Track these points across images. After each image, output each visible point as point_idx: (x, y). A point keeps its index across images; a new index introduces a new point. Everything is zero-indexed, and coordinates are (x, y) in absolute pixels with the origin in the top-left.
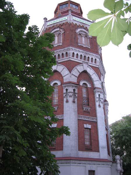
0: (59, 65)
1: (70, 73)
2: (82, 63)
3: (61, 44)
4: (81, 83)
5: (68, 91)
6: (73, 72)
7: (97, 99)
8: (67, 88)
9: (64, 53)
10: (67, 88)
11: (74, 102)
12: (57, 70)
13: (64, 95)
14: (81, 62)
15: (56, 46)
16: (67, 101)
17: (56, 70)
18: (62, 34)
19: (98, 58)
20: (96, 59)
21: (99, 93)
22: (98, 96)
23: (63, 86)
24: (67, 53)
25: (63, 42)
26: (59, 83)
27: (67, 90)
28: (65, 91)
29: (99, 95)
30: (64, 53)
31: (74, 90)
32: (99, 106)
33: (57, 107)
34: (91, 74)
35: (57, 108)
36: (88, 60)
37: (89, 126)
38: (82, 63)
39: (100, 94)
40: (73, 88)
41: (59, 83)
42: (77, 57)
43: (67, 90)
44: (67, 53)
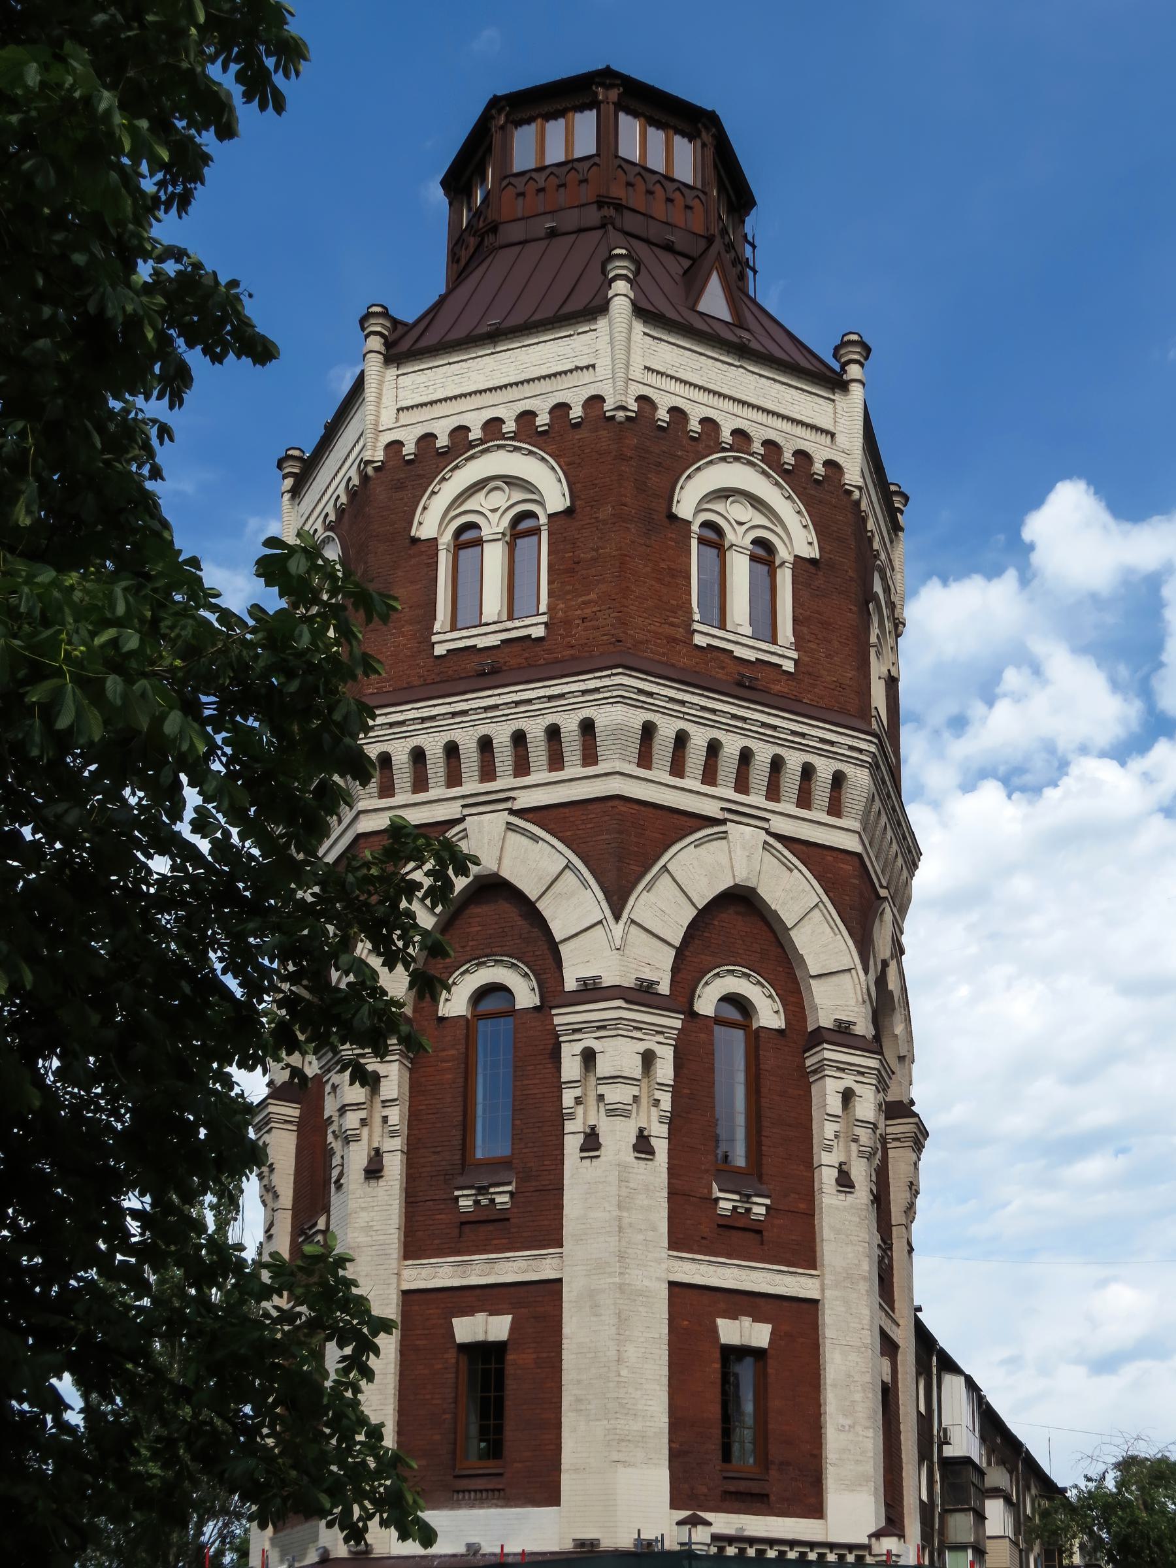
0: (524, 832)
1: (617, 918)
2: (723, 822)
3: (539, 632)
4: (707, 1002)
5: (603, 1067)
7: (830, 1129)
9: (570, 724)
11: (643, 1146)
12: (505, 874)
13: (568, 1098)
14: (710, 808)
15: (493, 640)
16: (591, 1142)
18: (543, 520)
19: (861, 764)
20: (838, 779)
21: (849, 1081)
22: (834, 1104)
23: (557, 1021)
24: (587, 727)
25: (551, 608)
26: (525, 995)
27: (589, 1057)
28: (571, 1067)
29: (848, 1096)
30: (570, 724)
31: (648, 1058)
32: (845, 1181)
34: (789, 920)
36: (773, 793)
37: (758, 1334)
38: (723, 822)
39: (858, 1089)
40: (641, 1047)
41: (525, 995)
42: (678, 768)
43: (589, 1057)
44: (587, 727)
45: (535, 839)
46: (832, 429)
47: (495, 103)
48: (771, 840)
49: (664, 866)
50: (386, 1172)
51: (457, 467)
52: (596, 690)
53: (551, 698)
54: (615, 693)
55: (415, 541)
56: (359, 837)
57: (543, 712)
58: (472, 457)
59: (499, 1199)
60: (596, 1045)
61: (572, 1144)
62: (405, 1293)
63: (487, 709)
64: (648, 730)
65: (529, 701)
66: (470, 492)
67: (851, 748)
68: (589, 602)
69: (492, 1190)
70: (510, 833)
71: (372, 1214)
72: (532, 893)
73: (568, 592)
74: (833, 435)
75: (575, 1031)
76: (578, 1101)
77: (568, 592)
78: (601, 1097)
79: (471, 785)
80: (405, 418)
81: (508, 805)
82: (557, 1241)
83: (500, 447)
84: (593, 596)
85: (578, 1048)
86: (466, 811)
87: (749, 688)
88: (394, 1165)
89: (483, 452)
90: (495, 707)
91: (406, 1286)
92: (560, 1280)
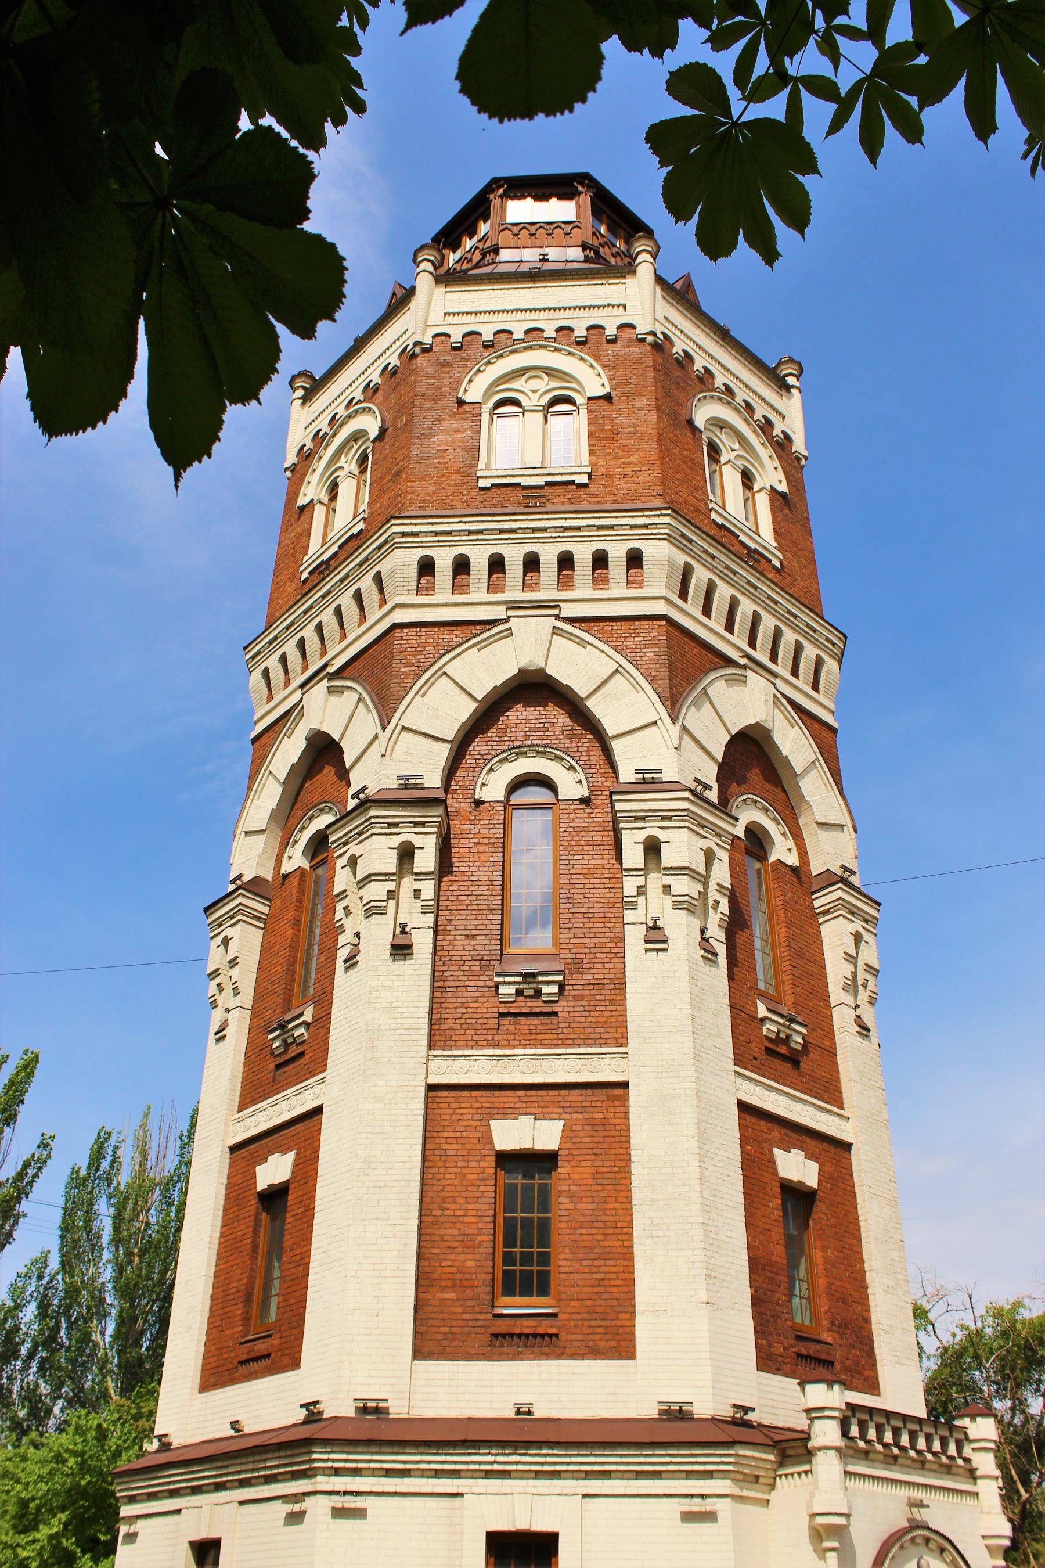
0: (570, 636)
2: (744, 667)
6: (696, 718)
8: (652, 829)
9: (617, 553)
10: (652, 829)
17: (541, 672)
27: (652, 848)
31: (709, 856)
33: (560, 978)
35: (555, 989)
40: (705, 844)
43: (652, 848)
44: (635, 559)
45: (583, 643)
46: (784, 412)
47: (495, 183)
48: (779, 695)
49: (704, 688)
50: (416, 949)
51: (501, 356)
52: (646, 526)
53: (600, 528)
54: (662, 531)
55: (461, 403)
56: (396, 626)
57: (590, 539)
58: (515, 351)
59: (546, 989)
60: (662, 835)
61: (634, 937)
62: (431, 1088)
63: (535, 530)
64: (687, 572)
65: (578, 528)
66: (514, 375)
67: (827, 639)
68: (629, 463)
69: (540, 979)
70: (555, 636)
71: (395, 994)
72: (581, 689)
73: (610, 454)
74: (784, 417)
75: (637, 819)
76: (641, 890)
77: (610, 454)
78: (667, 889)
79: (514, 592)
80: (450, 319)
81: (556, 612)
82: (622, 1040)
83: (541, 347)
84: (633, 459)
85: (641, 836)
86: (511, 613)
87: (751, 567)
88: (422, 942)
89: (526, 349)
90: (545, 529)
91: (433, 1080)
92: (625, 1085)
